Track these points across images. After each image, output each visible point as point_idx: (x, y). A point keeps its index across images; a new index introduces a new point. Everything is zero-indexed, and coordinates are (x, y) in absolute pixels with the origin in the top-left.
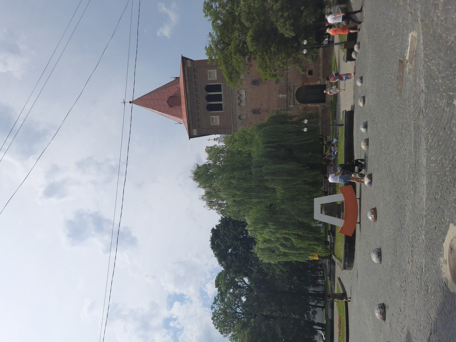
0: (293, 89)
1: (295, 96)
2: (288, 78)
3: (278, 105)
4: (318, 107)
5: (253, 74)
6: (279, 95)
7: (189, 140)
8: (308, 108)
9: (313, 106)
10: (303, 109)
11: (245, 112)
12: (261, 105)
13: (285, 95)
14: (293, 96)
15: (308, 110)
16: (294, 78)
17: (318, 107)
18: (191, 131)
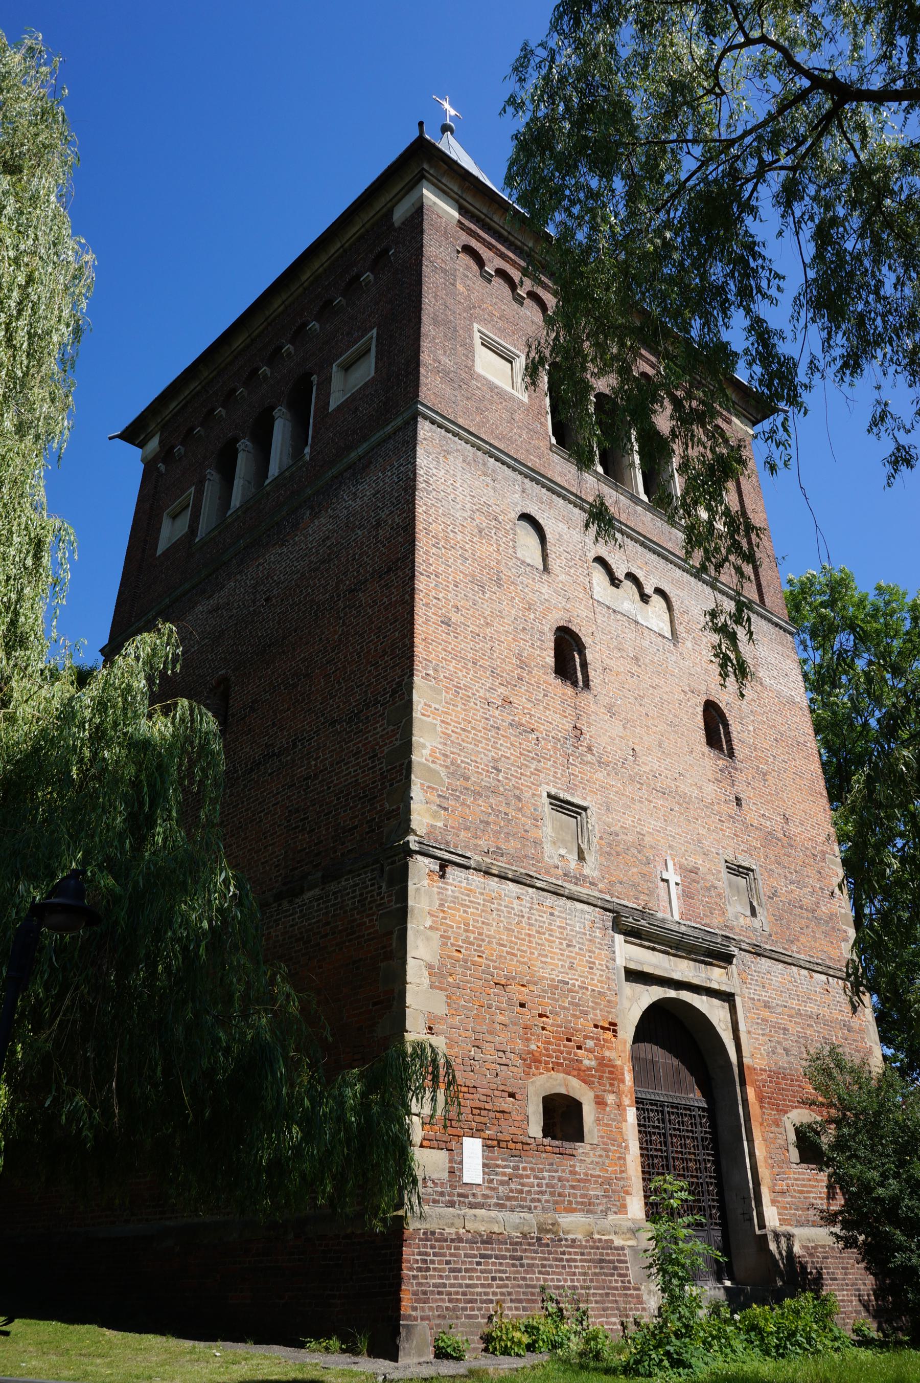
0: (715, 986)
1: (672, 994)
2: (764, 959)
3: (617, 835)
4: (628, 1198)
5: (751, 728)
6: (675, 865)
7: (421, 124)
8: (611, 1099)
9: (627, 1147)
10: (607, 1053)
11: (562, 577)
12: (611, 711)
13: (682, 914)
14: (676, 976)
15: (600, 1102)
16: (767, 1005)
17: (623, 1208)
18: (456, 189)
